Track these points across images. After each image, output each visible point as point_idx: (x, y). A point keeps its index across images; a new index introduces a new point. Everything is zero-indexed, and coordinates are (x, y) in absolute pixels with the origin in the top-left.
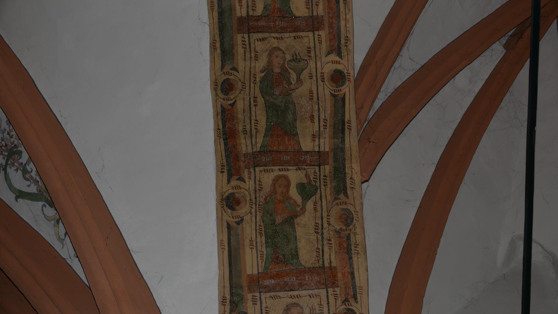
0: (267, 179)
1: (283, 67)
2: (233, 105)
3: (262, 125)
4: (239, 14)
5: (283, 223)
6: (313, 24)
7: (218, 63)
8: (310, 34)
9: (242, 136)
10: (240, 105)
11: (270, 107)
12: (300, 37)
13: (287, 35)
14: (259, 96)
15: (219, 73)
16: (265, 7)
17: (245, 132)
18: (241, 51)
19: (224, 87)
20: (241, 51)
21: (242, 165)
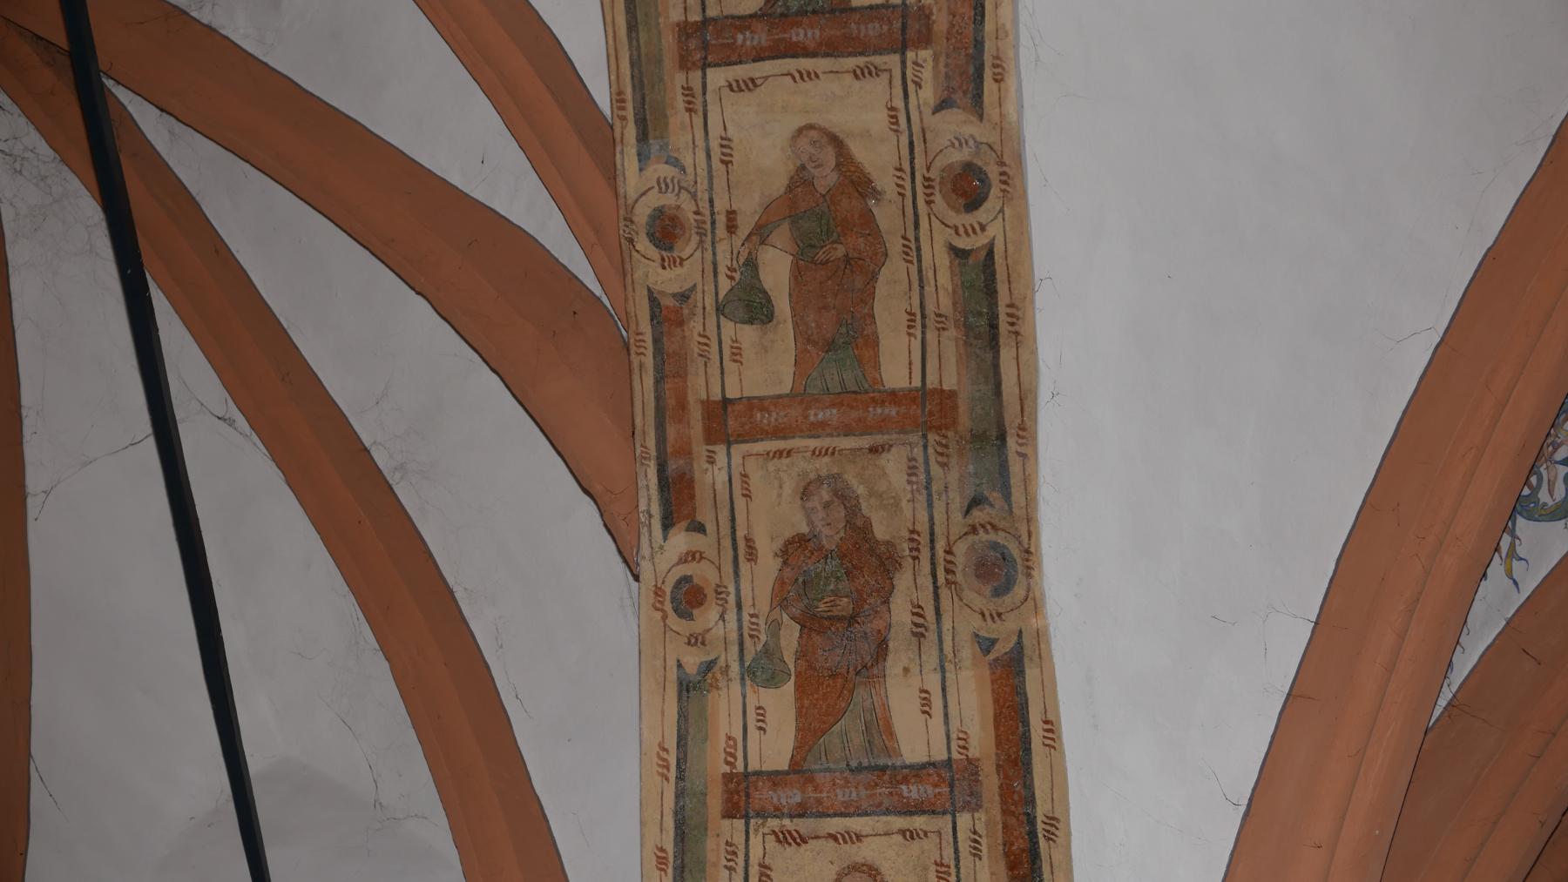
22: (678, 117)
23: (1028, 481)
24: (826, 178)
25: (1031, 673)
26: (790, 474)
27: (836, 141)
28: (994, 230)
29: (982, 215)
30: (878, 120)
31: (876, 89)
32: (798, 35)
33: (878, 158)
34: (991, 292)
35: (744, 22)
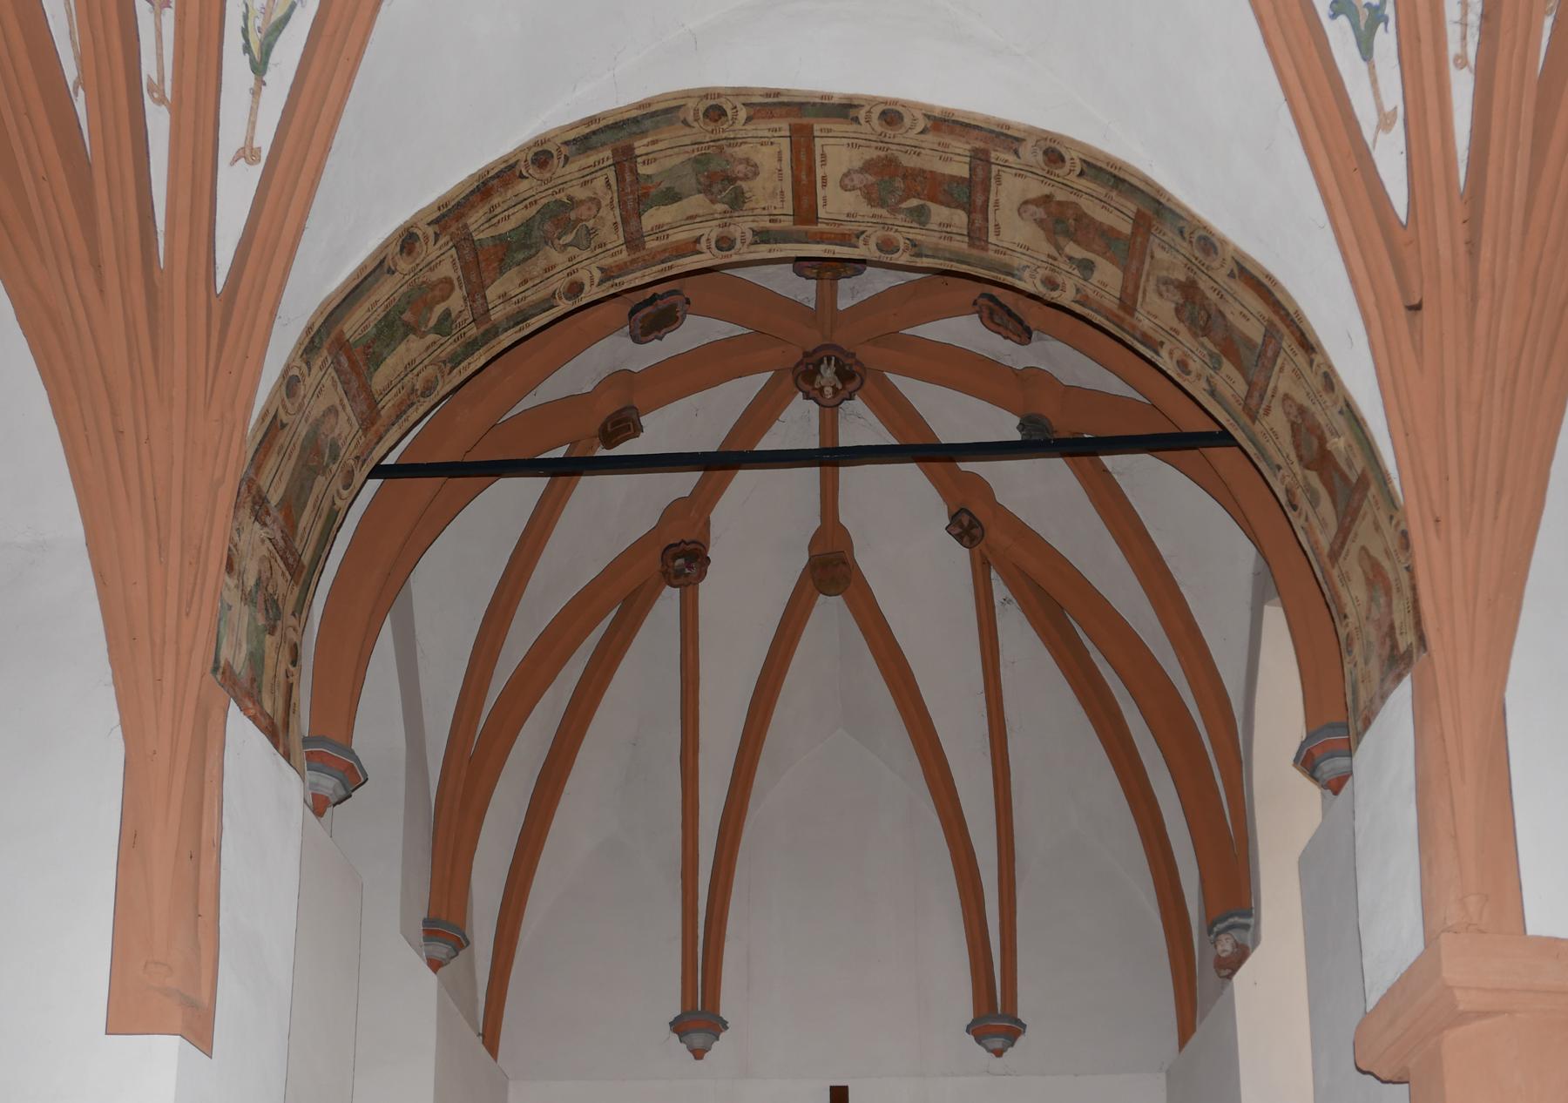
0: (447, 270)
1: (579, 220)
2: (522, 176)
3: (505, 227)
4: (636, 144)
5: (406, 324)
6: (634, 241)
7: (572, 135)
8: (622, 240)
9: (486, 209)
10: (523, 186)
11: (528, 225)
12: (616, 228)
13: (617, 212)
14: (538, 207)
15: (559, 141)
16: (649, 176)
17: (493, 208)
18: (591, 160)
19: (540, 155)
20: (591, 160)
21: (453, 229)
22: (1006, 259)
23: (1179, 205)
24: (1040, 213)
25: (1248, 266)
26: (1152, 296)
27: (1026, 202)
28: (1074, 155)
29: (1067, 157)
30: (1018, 180)
31: (1008, 179)
32: (979, 200)
33: (1036, 189)
34: (1101, 169)
35: (971, 222)
